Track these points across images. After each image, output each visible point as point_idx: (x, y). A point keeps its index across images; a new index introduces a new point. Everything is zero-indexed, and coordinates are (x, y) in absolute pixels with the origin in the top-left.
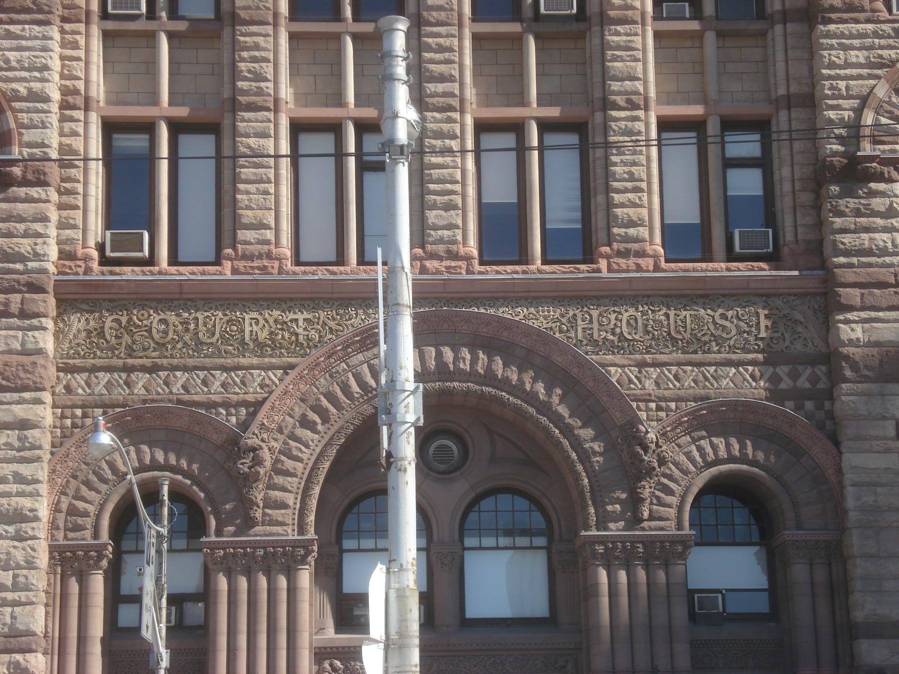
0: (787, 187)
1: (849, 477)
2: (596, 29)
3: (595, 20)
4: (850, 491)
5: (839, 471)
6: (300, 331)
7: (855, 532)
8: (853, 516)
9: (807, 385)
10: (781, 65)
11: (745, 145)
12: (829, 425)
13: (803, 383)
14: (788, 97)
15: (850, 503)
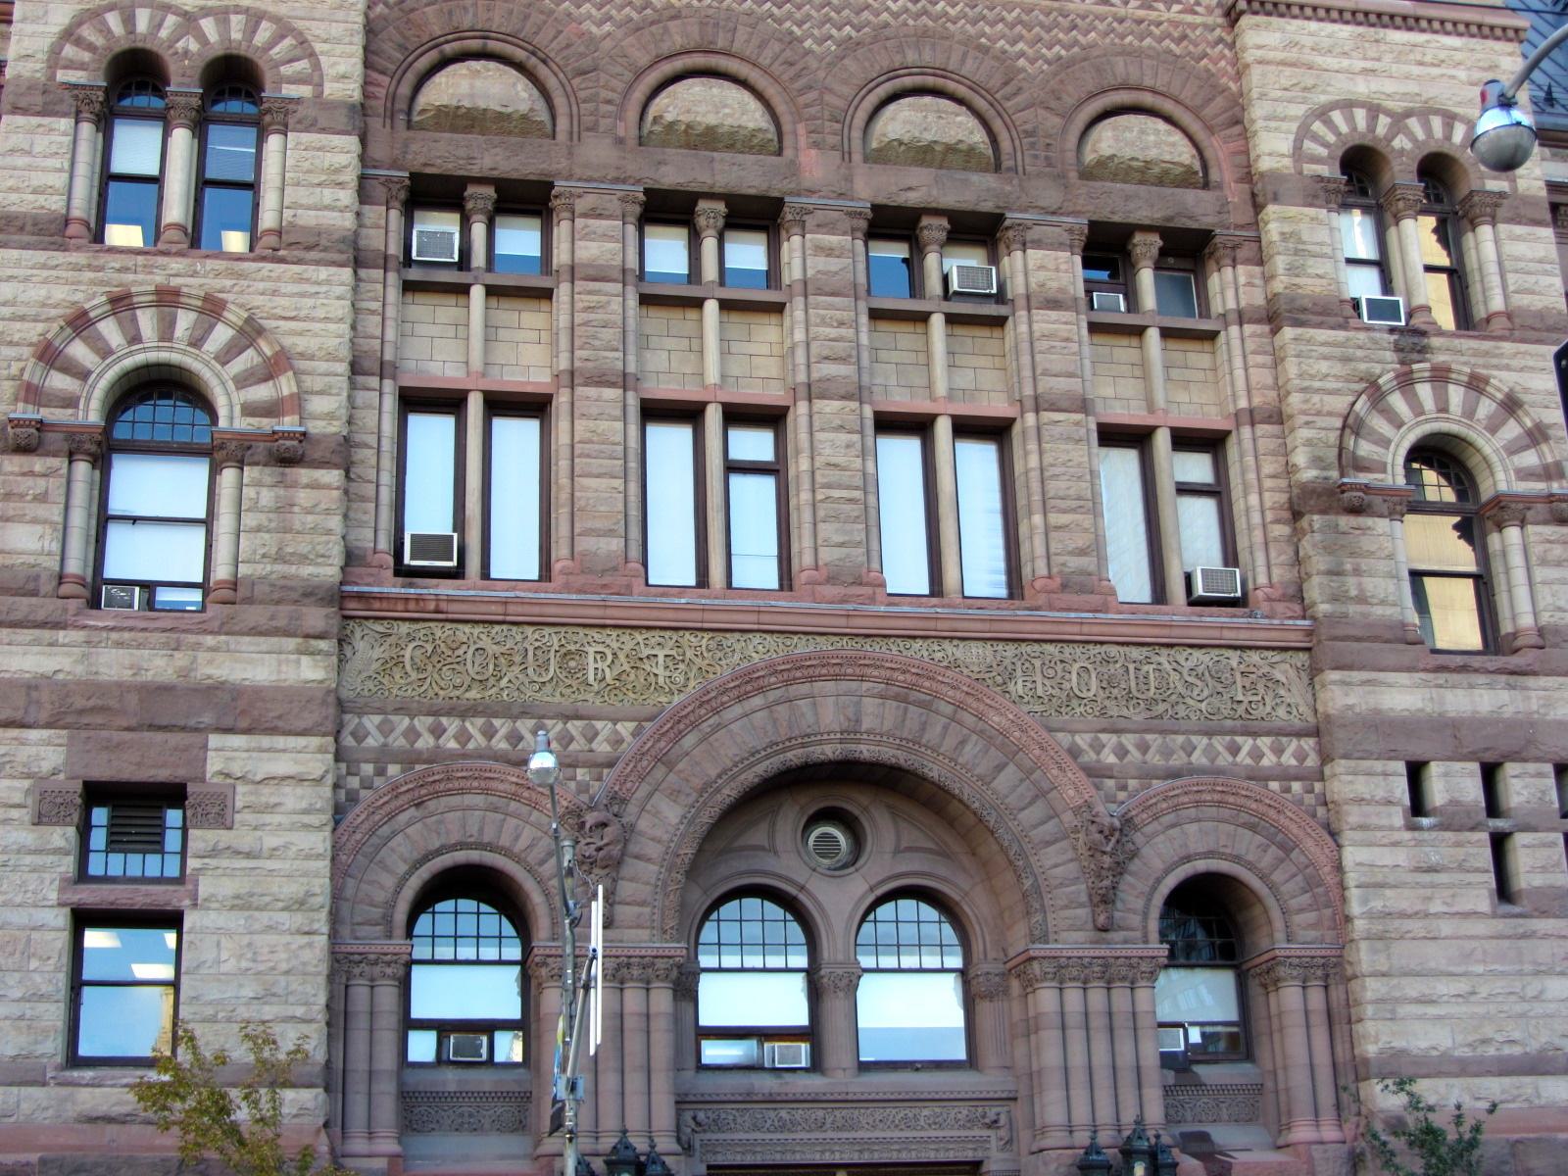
0: (1256, 518)
1: (1352, 878)
2: (1022, 314)
3: (1021, 302)
4: (1354, 894)
5: (1339, 868)
6: (660, 671)
7: (1363, 945)
8: (1360, 925)
9: (1293, 762)
10: (1239, 373)
11: (1196, 468)
12: (1321, 811)
13: (1288, 759)
14: (1251, 411)
15: (1355, 908)
